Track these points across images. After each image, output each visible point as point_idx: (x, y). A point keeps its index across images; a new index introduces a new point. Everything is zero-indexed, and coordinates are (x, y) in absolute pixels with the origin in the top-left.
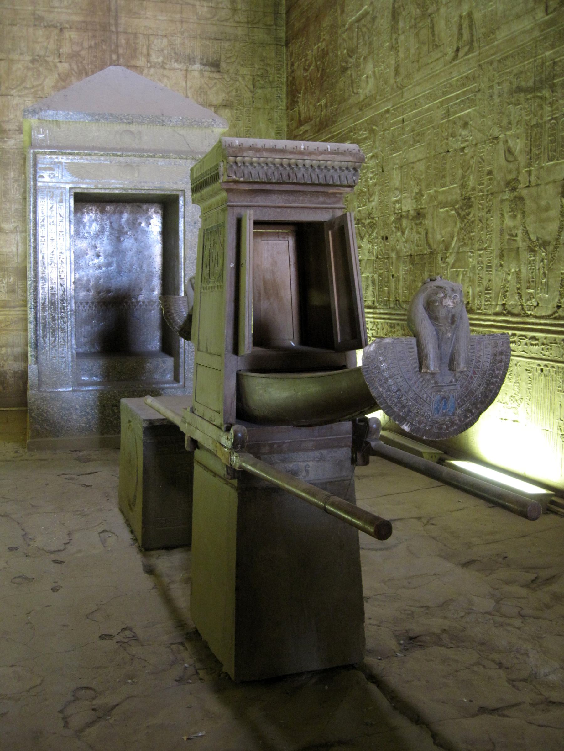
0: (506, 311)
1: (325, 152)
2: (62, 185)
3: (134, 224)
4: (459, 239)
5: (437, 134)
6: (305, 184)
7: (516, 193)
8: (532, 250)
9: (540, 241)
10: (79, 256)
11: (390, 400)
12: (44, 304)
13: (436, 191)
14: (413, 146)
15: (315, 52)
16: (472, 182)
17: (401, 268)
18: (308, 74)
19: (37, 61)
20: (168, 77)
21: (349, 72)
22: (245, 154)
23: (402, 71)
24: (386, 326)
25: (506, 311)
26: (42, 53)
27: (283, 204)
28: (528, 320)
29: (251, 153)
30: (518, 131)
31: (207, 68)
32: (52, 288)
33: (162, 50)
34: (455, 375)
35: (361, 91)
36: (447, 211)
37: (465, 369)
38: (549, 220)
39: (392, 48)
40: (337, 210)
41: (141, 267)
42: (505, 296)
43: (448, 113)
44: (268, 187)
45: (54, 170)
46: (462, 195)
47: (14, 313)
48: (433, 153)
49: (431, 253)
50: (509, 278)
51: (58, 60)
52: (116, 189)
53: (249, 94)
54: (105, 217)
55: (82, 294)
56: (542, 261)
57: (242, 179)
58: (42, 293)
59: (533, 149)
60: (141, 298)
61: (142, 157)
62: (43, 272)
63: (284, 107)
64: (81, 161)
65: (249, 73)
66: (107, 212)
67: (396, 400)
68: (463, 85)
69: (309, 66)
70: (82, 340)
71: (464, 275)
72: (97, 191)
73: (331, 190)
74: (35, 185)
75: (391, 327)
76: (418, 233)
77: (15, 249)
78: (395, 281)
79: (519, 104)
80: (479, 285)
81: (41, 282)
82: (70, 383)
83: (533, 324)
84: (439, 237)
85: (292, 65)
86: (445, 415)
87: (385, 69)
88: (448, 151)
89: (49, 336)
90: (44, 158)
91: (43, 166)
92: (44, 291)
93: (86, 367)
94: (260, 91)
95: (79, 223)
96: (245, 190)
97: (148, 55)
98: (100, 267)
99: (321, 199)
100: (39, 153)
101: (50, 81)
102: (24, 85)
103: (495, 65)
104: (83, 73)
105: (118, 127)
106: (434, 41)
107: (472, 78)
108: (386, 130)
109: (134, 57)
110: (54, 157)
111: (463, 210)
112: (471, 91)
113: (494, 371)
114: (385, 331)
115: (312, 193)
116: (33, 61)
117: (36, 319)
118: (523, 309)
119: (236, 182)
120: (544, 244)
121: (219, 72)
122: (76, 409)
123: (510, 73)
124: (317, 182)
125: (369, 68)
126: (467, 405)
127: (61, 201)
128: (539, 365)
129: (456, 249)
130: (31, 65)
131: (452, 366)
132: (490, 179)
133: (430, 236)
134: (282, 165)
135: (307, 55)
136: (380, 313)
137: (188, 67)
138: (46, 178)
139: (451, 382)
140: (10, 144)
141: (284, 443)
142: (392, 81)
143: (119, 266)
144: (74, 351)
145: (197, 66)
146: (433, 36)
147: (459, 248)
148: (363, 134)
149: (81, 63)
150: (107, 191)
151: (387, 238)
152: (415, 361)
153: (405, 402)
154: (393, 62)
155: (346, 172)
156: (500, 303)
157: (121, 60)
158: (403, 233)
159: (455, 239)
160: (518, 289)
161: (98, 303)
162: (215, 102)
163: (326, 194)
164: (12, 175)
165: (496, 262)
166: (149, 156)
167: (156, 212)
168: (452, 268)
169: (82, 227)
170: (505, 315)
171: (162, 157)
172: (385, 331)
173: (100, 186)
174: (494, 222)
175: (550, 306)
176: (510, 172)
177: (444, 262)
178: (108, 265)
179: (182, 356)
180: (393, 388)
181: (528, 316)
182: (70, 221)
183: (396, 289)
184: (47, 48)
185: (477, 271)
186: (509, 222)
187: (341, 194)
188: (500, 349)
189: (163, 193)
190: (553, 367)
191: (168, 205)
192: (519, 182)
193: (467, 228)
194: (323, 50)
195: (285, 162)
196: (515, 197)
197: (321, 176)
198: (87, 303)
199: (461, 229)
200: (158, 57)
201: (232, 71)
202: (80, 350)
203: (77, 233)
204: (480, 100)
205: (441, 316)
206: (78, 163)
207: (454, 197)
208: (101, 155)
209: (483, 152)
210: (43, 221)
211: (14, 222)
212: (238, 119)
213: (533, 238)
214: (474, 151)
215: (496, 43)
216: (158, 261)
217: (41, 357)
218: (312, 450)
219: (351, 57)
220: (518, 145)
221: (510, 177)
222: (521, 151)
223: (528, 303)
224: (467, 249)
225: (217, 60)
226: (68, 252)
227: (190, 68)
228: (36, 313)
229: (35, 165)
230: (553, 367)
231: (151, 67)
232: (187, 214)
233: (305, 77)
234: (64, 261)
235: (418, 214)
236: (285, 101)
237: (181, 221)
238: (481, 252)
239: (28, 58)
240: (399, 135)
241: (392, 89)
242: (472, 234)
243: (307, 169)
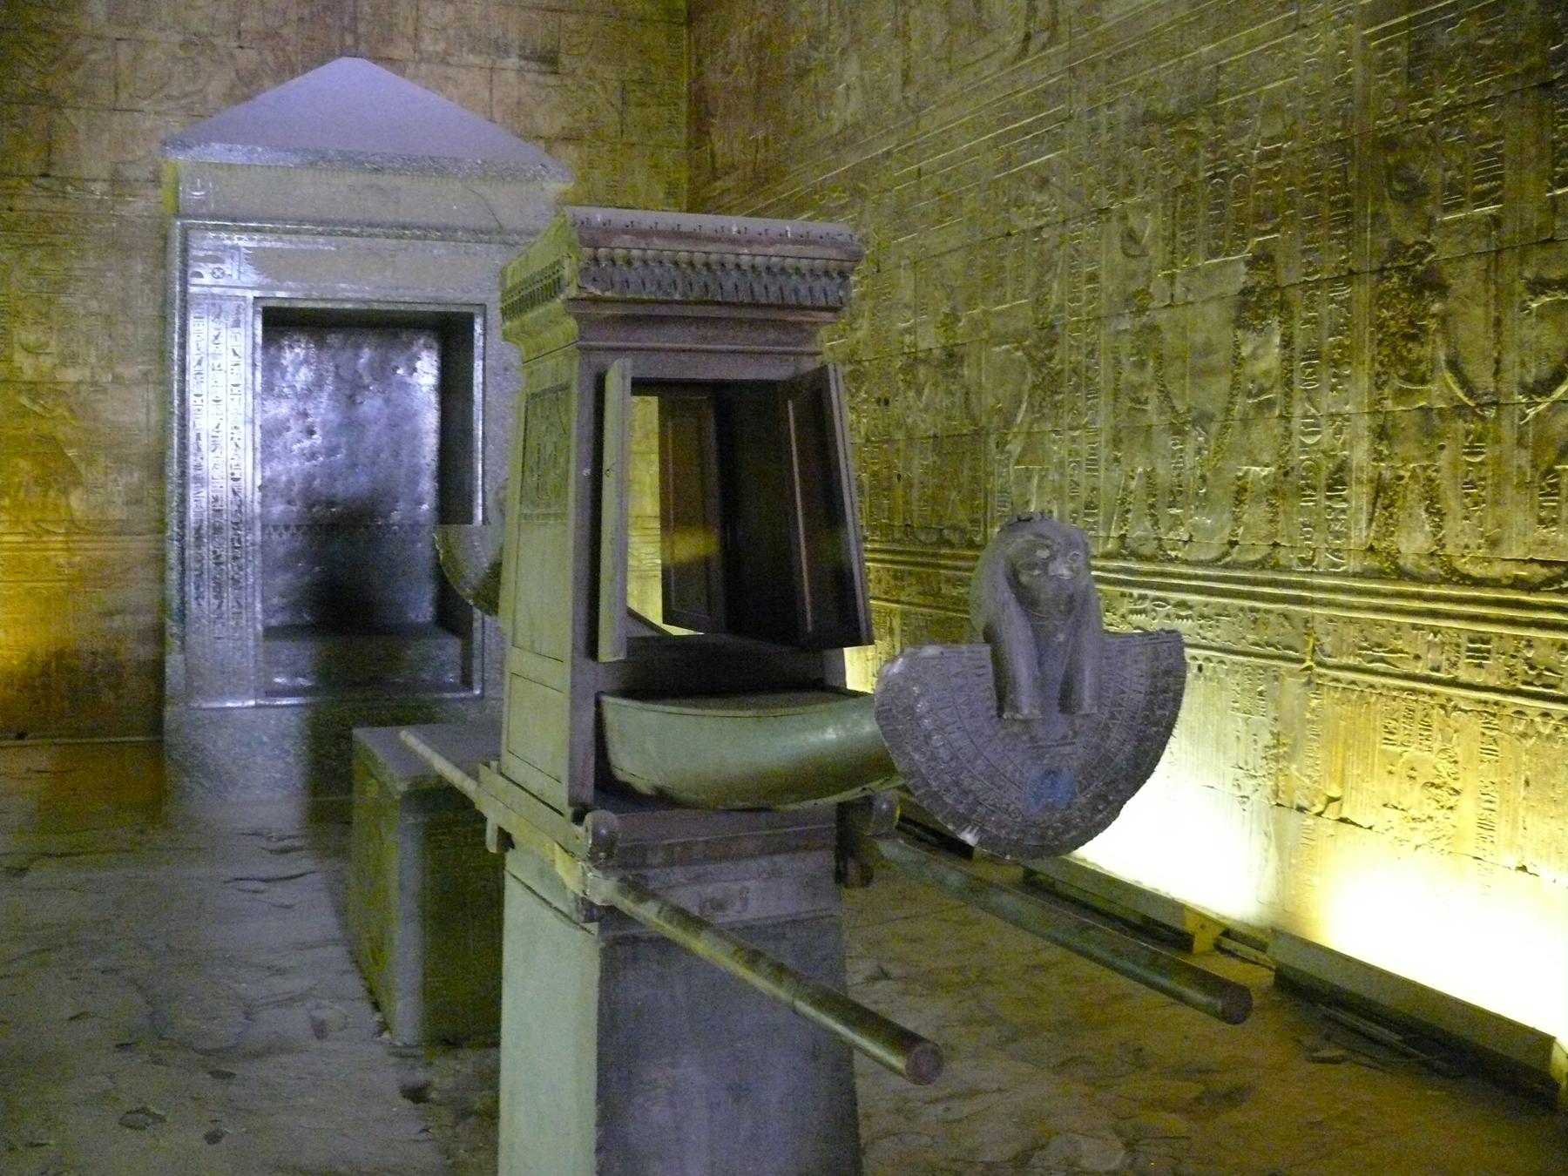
0: (1125, 549)
1: (782, 238)
2: (238, 292)
3: (383, 369)
4: (1031, 405)
5: (986, 201)
6: (741, 305)
7: (1144, 319)
8: (1178, 431)
9: (1194, 413)
10: (271, 433)
11: (936, 778)
12: (198, 530)
13: (985, 312)
14: (941, 222)
15: (745, 38)
16: (1056, 293)
17: (916, 462)
18: (730, 79)
21: (812, 78)
22: (615, 242)
23: (918, 78)
24: (886, 577)
25: (1125, 549)
27: (695, 346)
28: (1170, 568)
29: (627, 239)
30: (1148, 198)
31: (533, 65)
32: (216, 500)
33: (444, 29)
34: (1072, 724)
35: (834, 113)
36: (1008, 351)
37: (1095, 710)
38: (1212, 371)
39: (896, 33)
40: (805, 358)
41: (396, 454)
42: (1125, 521)
43: (1008, 162)
44: (664, 311)
45: (222, 262)
46: (1037, 321)
47: (139, 546)
48: (979, 237)
49: (976, 433)
50: (1133, 484)
51: (235, 44)
52: (348, 300)
53: (616, 117)
54: (325, 357)
55: (278, 509)
56: (1199, 451)
57: (608, 294)
58: (192, 515)
59: (1179, 234)
60: (396, 516)
62: (198, 467)
63: (684, 144)
64: (279, 245)
65: (613, 76)
66: (330, 347)
67: (947, 779)
68: (1039, 107)
69: (733, 64)
70: (275, 601)
71: (1042, 478)
72: (310, 305)
74: (184, 292)
75: (895, 578)
76: (951, 393)
77: (142, 417)
78: (905, 487)
79: (1149, 145)
80: (1072, 498)
81: (192, 485)
82: (252, 692)
83: (1181, 576)
84: (991, 401)
85: (700, 62)
86: (1052, 808)
87: (884, 72)
88: (1009, 234)
89: (209, 594)
90: (204, 238)
91: (202, 254)
92: (199, 502)
93: (283, 657)
94: (634, 111)
95: (272, 367)
96: (614, 317)
97: (417, 37)
98: (313, 455)
99: (772, 335)
100: (192, 227)
101: (217, 85)
102: (166, 91)
103: (1102, 68)
104: (287, 69)
105: (352, 178)
106: (980, 20)
107: (1057, 94)
108: (886, 190)
109: (388, 41)
110: (224, 235)
111: (1041, 350)
112: (1055, 118)
113: (1152, 711)
114: (884, 584)
115: (752, 322)
116: (184, 45)
117: (182, 562)
118: (1160, 547)
119: (596, 300)
120: (1203, 419)
121: (556, 73)
122: (262, 743)
123: (1132, 84)
124: (763, 300)
125: (852, 70)
126: (1097, 786)
127: (237, 324)
128: (1194, 658)
129: (1026, 426)
130: (181, 54)
131: (1066, 700)
132: (1094, 290)
133: (973, 397)
134: (691, 264)
135: (728, 45)
136: (873, 551)
137: (494, 62)
138: (205, 279)
139: (1065, 737)
140: (137, 207)
141: (697, 843)
142: (896, 97)
143: (351, 453)
144: (259, 627)
145: (513, 61)
146: (979, 11)
147: (1031, 425)
148: (839, 198)
149: (283, 50)
150: (329, 306)
151: (887, 403)
152: (987, 694)
153: (966, 782)
154: (898, 61)
155: (824, 280)
156: (1114, 534)
157: (363, 47)
158: (919, 393)
159: (1024, 406)
160: (1152, 506)
161: (310, 527)
162: (546, 132)
163: (784, 326)
164: (139, 268)
165: (1104, 453)
167: (427, 347)
168: (1018, 463)
169: (278, 375)
170: (1124, 558)
171: (442, 239)
172: (884, 584)
173: (315, 294)
174: (1102, 376)
175: (1216, 541)
176: (1133, 276)
177: (1002, 452)
178: (332, 451)
179: (477, 636)
180: (943, 753)
181: (1172, 560)
182: (254, 365)
183: (906, 502)
185: (1069, 471)
186: (1130, 376)
188: (1164, 665)
189: (441, 309)
190: (1222, 662)
191: (451, 333)
192: (1152, 297)
193: (1050, 384)
194: (760, 34)
195: (699, 258)
196: (1144, 326)
197: (772, 289)
198: (287, 528)
199: (1035, 387)
200: (436, 41)
201: (579, 71)
202: (273, 622)
203: (269, 386)
204: (1071, 135)
205: (1043, 597)
206: (271, 249)
207: (1021, 324)
208: (321, 234)
209: (1077, 237)
210: (199, 363)
211: (143, 363)
212: (591, 165)
213: (1181, 408)
214: (1061, 236)
215: (1101, 28)
216: (430, 443)
217: (192, 639)
218: (752, 856)
219: (816, 49)
220: (1149, 226)
221: (1133, 288)
222: (1154, 235)
223: (1171, 535)
224: (1048, 427)
225: (550, 51)
226: (250, 427)
227: (497, 66)
228: (182, 550)
229: (185, 250)
230: (1222, 662)
231: (421, 60)
232: (489, 352)
233: (725, 86)
234: (241, 444)
235: (951, 356)
236: (685, 130)
237: (478, 365)
238: (1077, 433)
239: (177, 38)
240: (912, 200)
241: (898, 112)
242: (1058, 398)
243: (744, 273)
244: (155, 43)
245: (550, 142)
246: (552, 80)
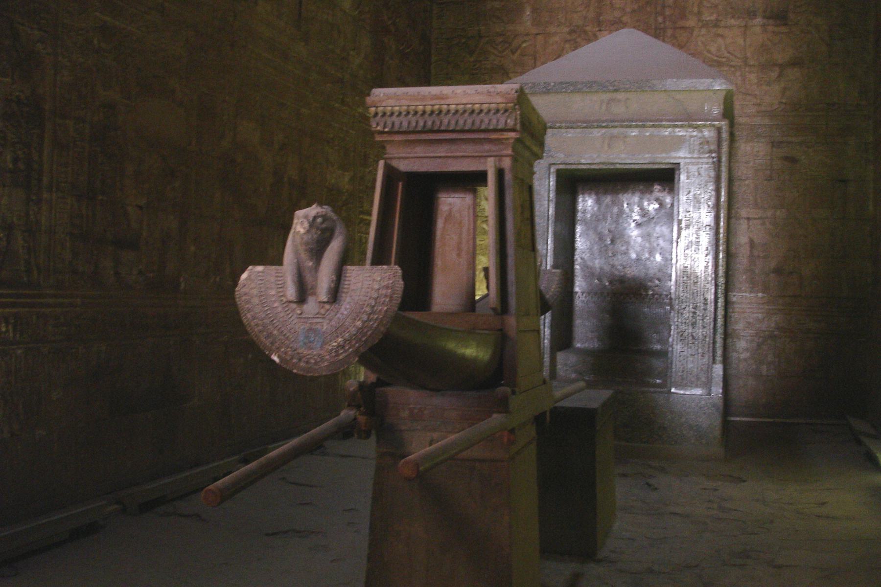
19: (575, 32)
20: (722, 36)
26: (580, 23)
31: (771, 22)
57: (386, 130)
61: (630, 127)
73: (494, 136)
97: (699, 13)
109: (683, 16)
116: (571, 32)
121: (786, 25)
145: (759, 21)
157: (667, 23)
161: (602, 293)
166: (637, 126)
171: (653, 126)
184: (585, 18)
187: (507, 139)
189: (656, 167)
195: (429, 108)
239: (566, 30)
244: (555, 34)
245: (781, 66)
246: (784, 29)
